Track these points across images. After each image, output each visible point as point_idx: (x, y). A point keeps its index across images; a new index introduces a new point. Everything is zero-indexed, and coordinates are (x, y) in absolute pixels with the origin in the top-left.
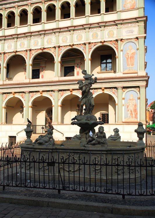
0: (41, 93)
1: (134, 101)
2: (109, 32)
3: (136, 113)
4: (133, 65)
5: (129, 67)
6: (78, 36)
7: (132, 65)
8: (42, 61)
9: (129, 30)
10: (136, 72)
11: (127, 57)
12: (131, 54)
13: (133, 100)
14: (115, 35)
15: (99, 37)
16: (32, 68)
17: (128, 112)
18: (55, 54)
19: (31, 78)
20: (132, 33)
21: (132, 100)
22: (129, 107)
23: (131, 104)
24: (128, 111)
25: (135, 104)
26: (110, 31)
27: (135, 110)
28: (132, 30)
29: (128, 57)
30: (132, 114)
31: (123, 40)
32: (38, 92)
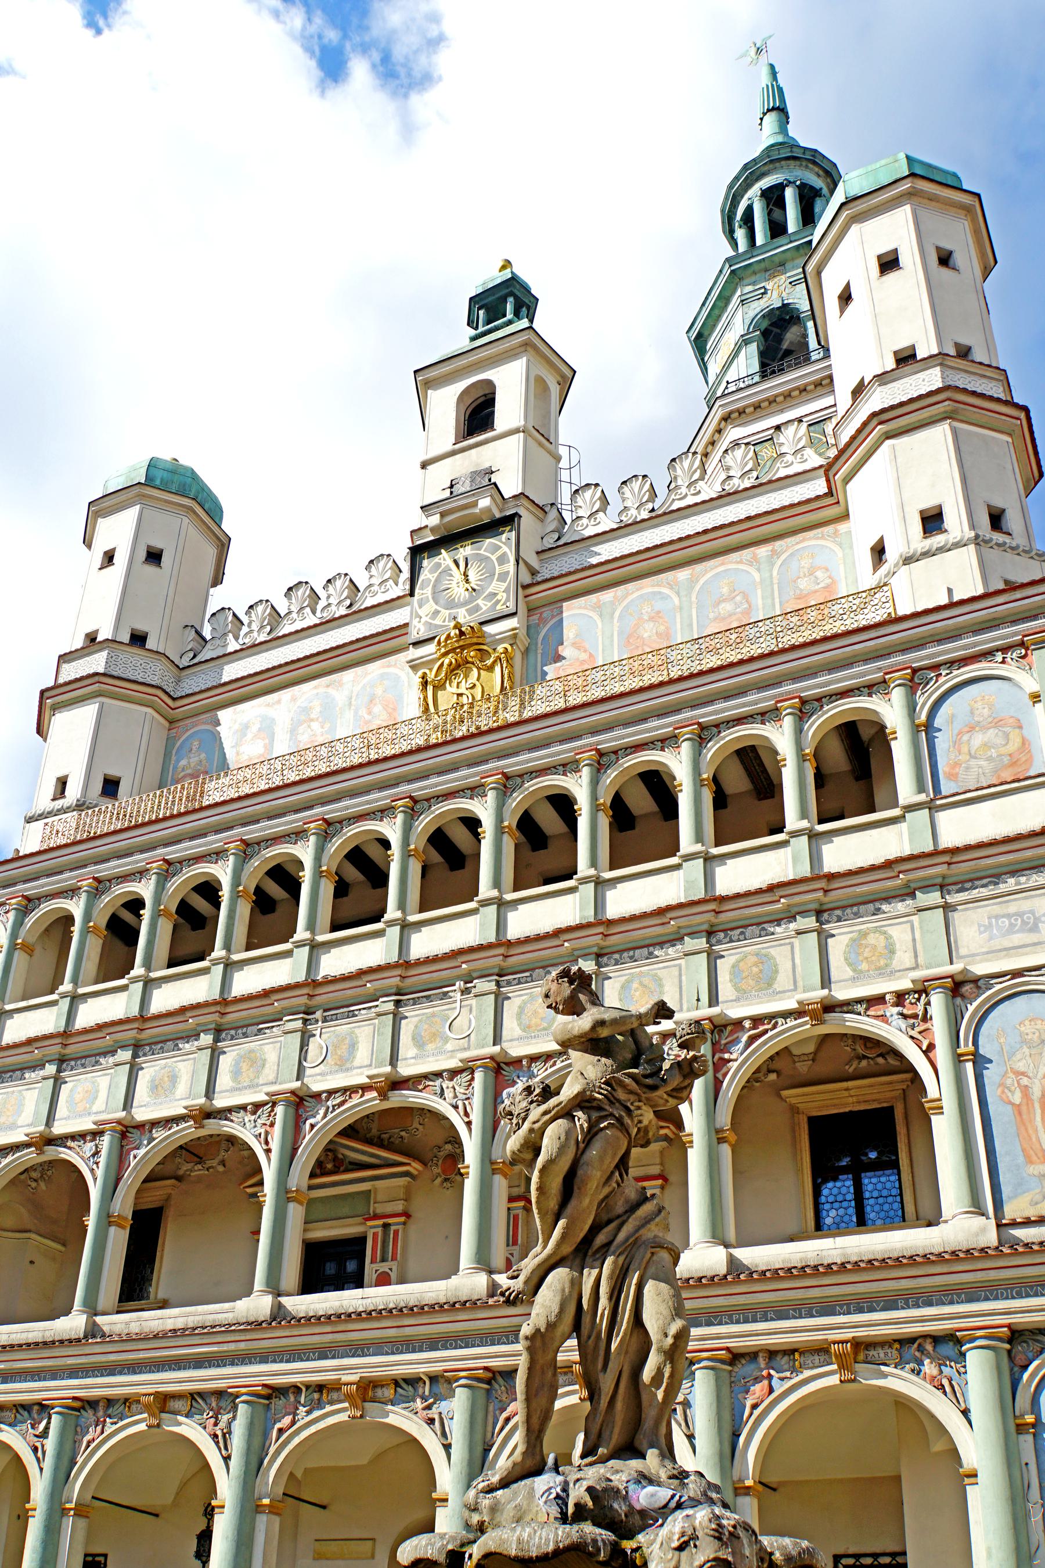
2: (853, 940)
6: (635, 985)
9: (1008, 916)
11: (1017, 1098)
14: (903, 958)
15: (783, 980)
20: (1034, 929)
26: (864, 935)
28: (1032, 912)
29: (1025, 1090)
31: (966, 989)
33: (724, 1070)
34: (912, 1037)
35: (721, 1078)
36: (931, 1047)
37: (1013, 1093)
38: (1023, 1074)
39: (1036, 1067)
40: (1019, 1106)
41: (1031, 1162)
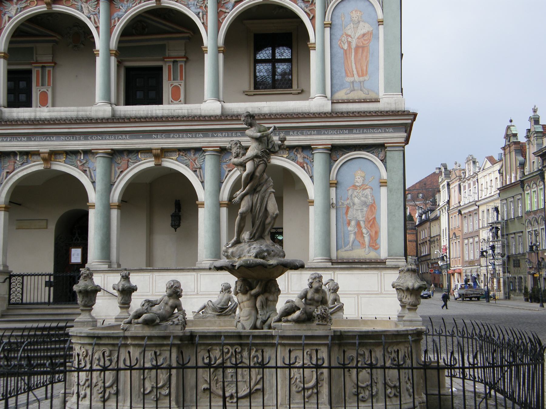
0: (45, 160)
1: (368, 191)
3: (374, 232)
4: (363, 76)
5: (352, 79)
7: (362, 74)
8: (37, 42)
10: (373, 96)
11: (346, 47)
12: (358, 38)
13: (363, 187)
16: (9, 64)
17: (349, 228)
18: (95, 22)
19: (6, 104)
21: (360, 187)
22: (350, 213)
23: (356, 200)
24: (349, 224)
25: (370, 200)
27: (373, 223)
29: (349, 43)
30: (362, 233)
32: (36, 153)
33: (223, 16)
34: (306, 12)
35: (221, 21)
36: (314, 17)
37: (344, 44)
38: (350, 36)
39: (355, 33)
40: (346, 50)
41: (348, 76)
